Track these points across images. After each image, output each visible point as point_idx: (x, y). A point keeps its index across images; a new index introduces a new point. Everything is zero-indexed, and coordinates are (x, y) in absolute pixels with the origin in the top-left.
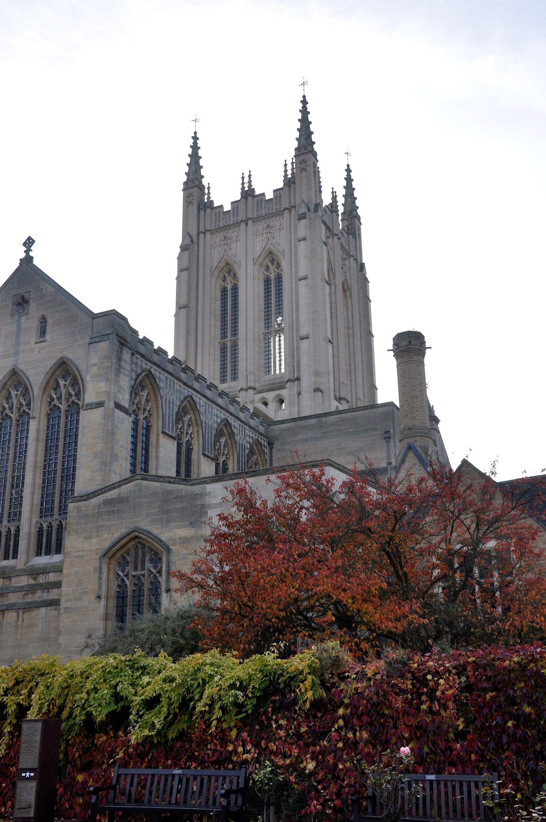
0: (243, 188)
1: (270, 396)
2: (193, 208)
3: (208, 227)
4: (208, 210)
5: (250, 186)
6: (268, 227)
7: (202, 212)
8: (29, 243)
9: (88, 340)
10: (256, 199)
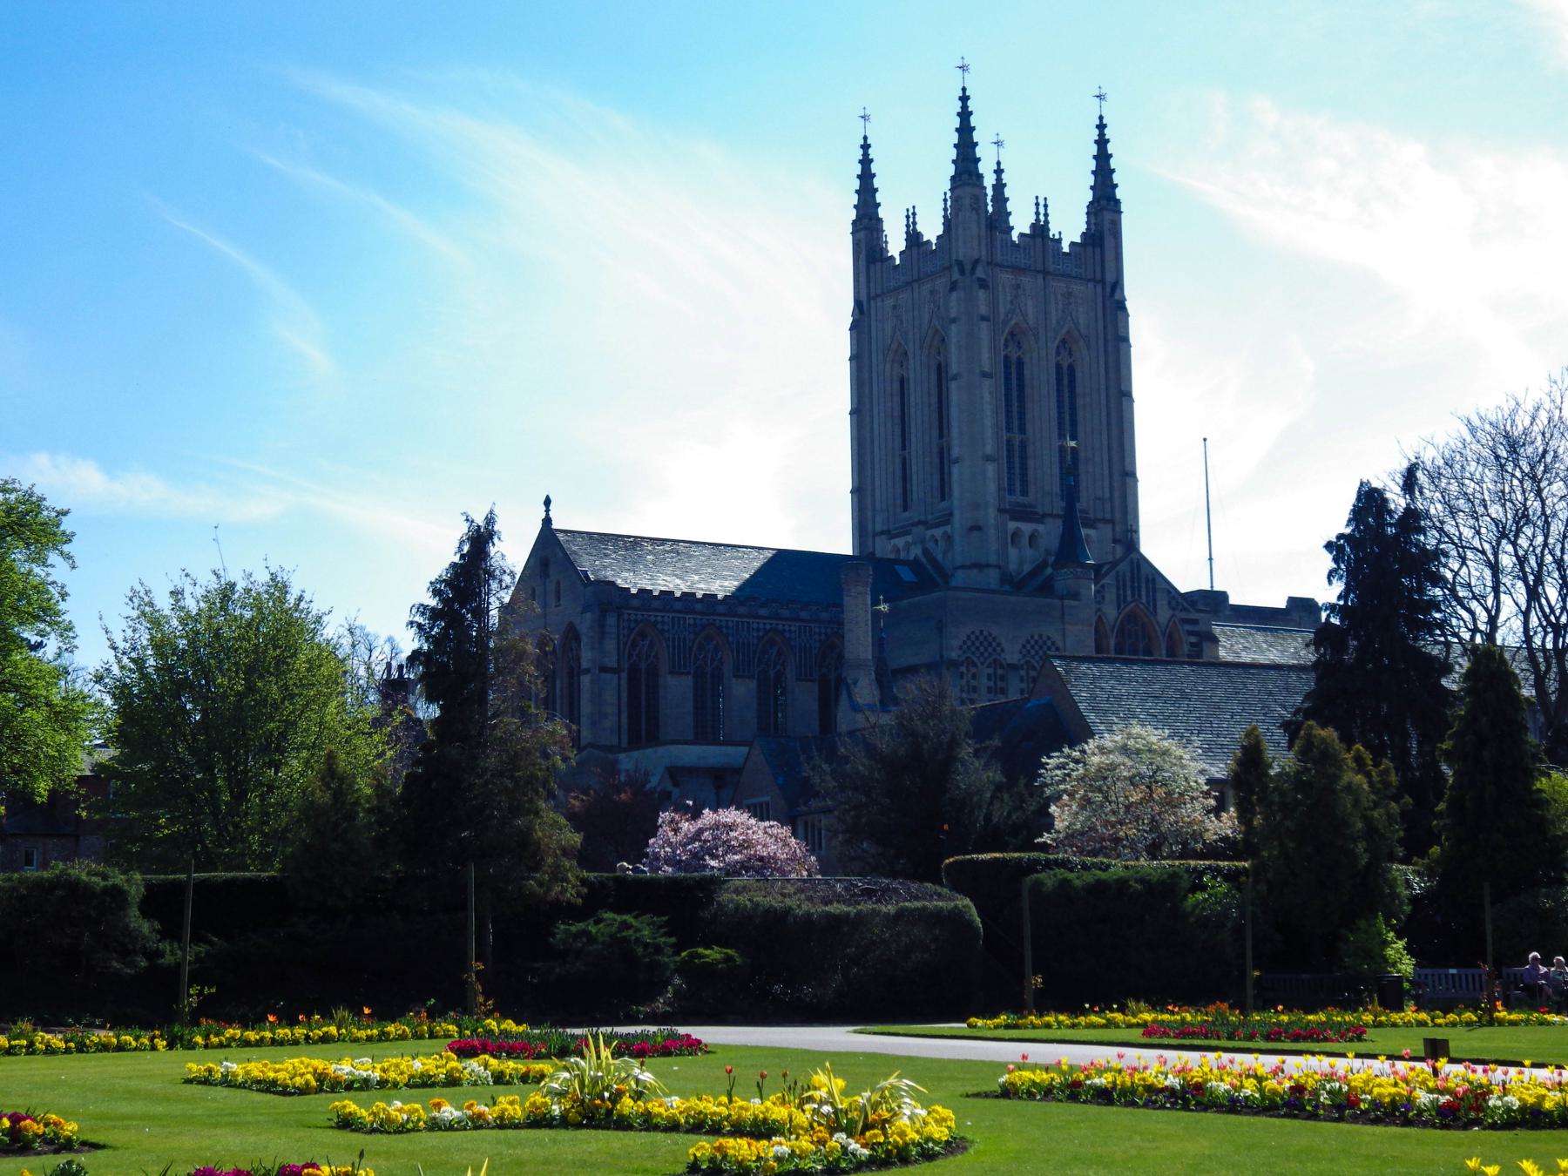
0: (907, 233)
1: (938, 532)
2: (862, 263)
3: (879, 292)
4: (878, 264)
5: (914, 229)
6: (932, 292)
7: (872, 266)
8: (547, 502)
9: (580, 609)
10: (921, 250)
